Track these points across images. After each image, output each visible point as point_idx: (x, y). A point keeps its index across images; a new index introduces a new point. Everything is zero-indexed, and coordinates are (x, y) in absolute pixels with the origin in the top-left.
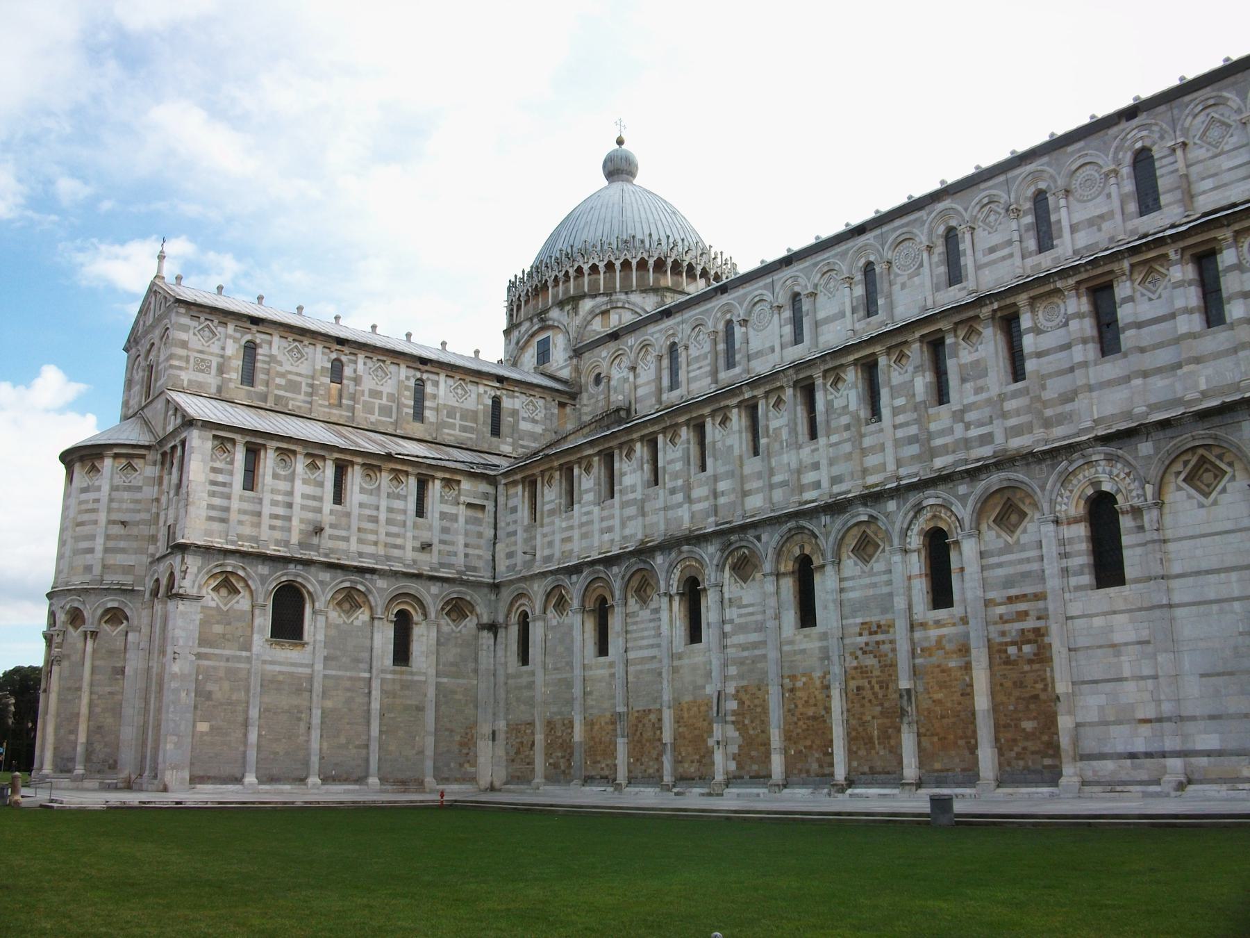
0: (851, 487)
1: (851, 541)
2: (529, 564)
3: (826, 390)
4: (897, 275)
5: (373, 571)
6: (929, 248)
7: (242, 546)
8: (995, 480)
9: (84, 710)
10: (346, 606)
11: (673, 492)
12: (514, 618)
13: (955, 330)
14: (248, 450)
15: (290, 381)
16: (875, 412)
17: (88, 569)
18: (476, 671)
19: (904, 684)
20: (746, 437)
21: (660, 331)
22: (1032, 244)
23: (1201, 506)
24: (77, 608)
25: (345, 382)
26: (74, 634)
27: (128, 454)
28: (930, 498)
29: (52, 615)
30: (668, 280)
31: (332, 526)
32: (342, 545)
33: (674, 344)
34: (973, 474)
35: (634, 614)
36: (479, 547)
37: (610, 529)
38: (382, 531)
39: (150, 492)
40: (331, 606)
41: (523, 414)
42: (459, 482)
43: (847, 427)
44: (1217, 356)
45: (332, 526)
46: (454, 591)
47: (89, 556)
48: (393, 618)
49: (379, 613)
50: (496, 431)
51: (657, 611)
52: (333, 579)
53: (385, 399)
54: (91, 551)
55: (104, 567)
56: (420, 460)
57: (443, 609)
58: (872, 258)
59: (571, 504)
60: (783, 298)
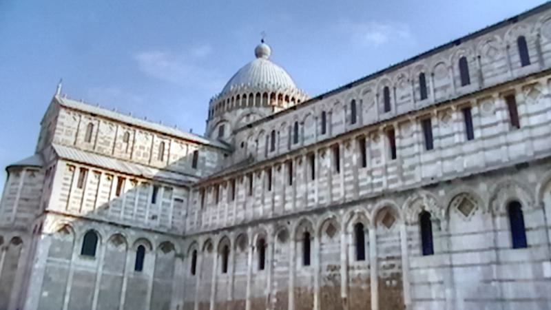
0: (326, 202)
1: (325, 227)
2: (199, 228)
3: (319, 158)
4: (364, 107)
5: (129, 227)
8: (382, 203)
10: (116, 242)
11: (257, 199)
12: (191, 253)
13: (369, 135)
14: (81, 171)
16: (338, 169)
20: (287, 176)
22: (418, 96)
23: (464, 220)
27: (32, 169)
28: (357, 209)
30: (276, 102)
31: (114, 206)
32: (117, 215)
34: (374, 199)
35: (238, 254)
36: (178, 218)
37: (231, 214)
38: (135, 210)
39: (39, 186)
41: (207, 158)
42: (172, 189)
43: (326, 175)
44: (470, 153)
45: (114, 206)
46: (165, 239)
47: (10, 213)
48: (136, 248)
49: (130, 245)
50: (195, 165)
51: (247, 254)
57: (160, 246)
58: (355, 98)
59: (217, 202)
60: (318, 113)
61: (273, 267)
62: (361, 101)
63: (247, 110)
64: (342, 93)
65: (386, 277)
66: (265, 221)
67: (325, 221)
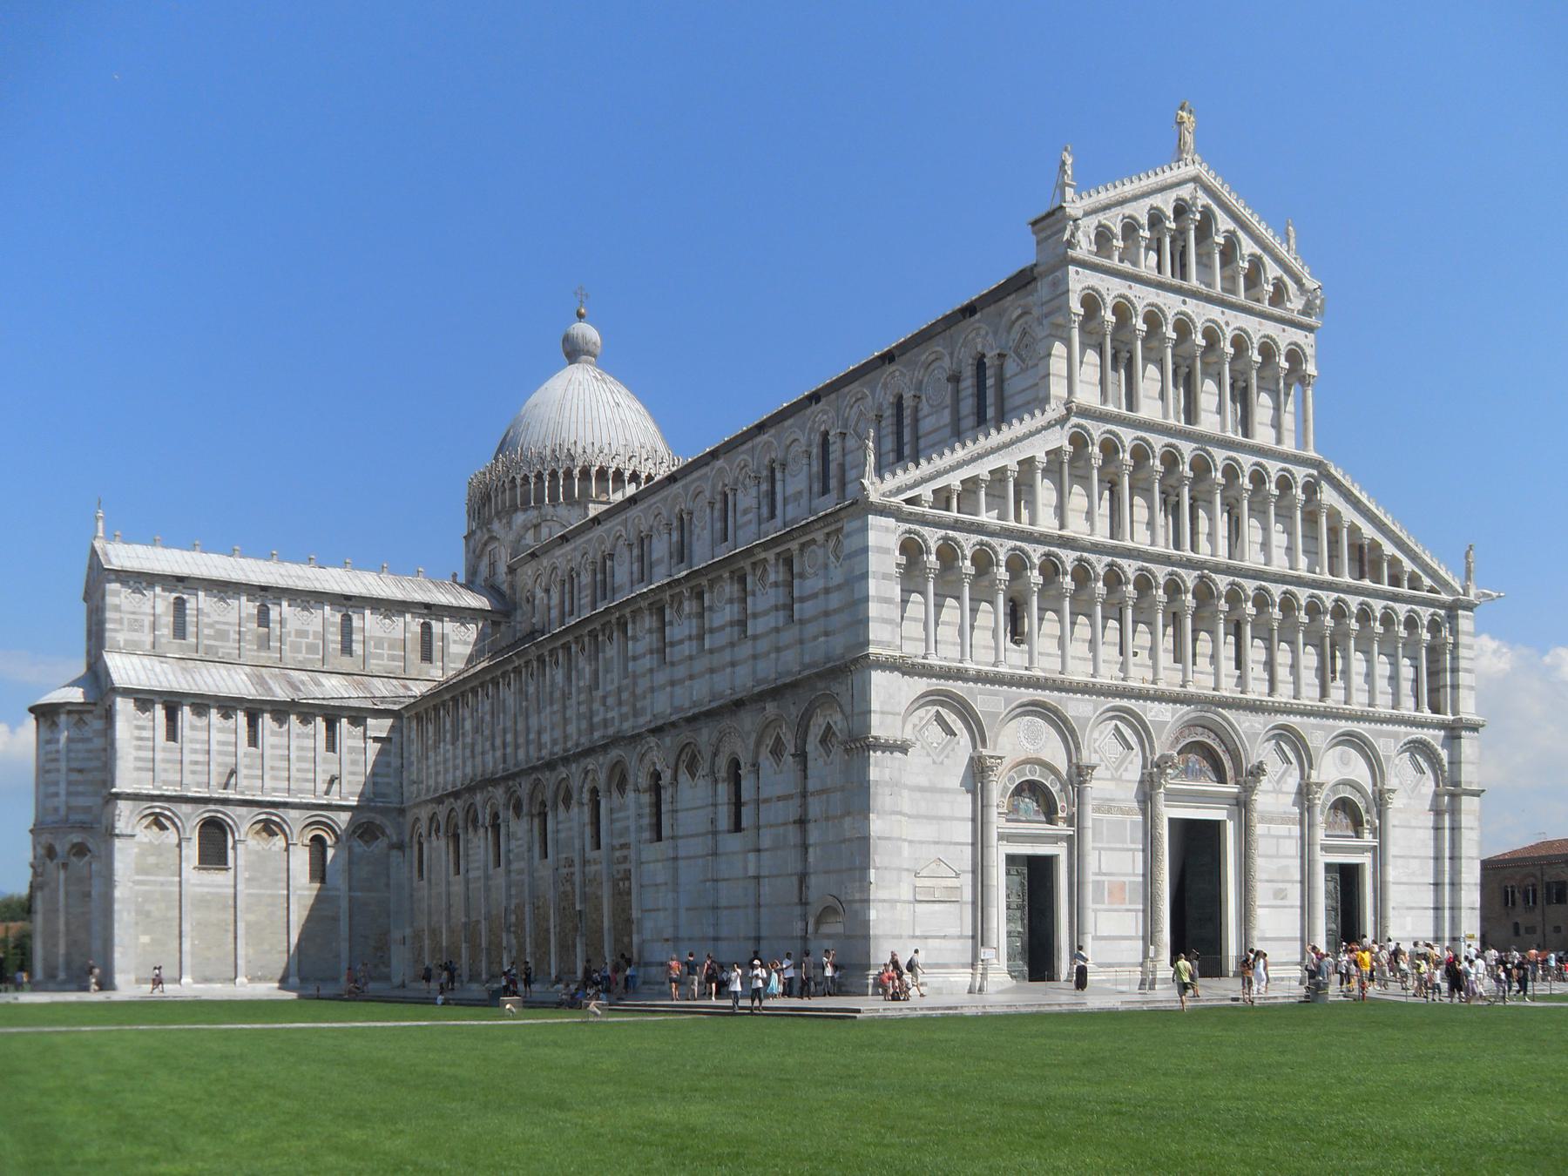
6: (712, 504)
7: (167, 790)
8: (614, 753)
9: (62, 927)
12: (415, 839)
15: (218, 631)
17: (56, 810)
18: (388, 885)
19: (578, 907)
21: (562, 555)
22: (765, 511)
23: (691, 787)
24: (51, 845)
25: (271, 625)
26: (50, 865)
29: (35, 848)
33: (572, 569)
36: (387, 776)
39: (98, 743)
40: (250, 836)
41: (452, 637)
47: (56, 799)
48: (307, 842)
50: (427, 656)
52: (249, 813)
53: (311, 637)
54: (56, 795)
55: (69, 808)
56: (325, 702)
57: (354, 832)
58: (683, 507)
60: (633, 538)
61: (509, 862)
62: (690, 513)
63: (533, 514)
64: (664, 493)
65: (619, 877)
66: (492, 781)
67: (560, 783)
